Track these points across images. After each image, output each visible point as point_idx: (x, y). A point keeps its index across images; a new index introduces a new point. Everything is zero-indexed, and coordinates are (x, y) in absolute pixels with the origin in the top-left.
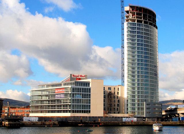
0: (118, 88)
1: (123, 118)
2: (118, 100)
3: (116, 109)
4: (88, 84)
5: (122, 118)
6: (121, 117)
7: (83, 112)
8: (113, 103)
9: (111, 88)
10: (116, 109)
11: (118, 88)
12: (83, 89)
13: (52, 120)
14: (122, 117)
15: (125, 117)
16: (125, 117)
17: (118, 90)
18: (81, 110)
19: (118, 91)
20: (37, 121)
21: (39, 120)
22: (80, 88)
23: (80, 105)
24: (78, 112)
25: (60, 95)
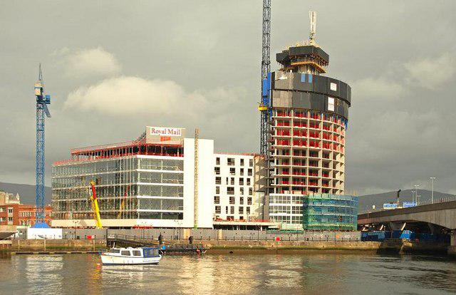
3: (245, 210)
4: (176, 150)
8: (237, 194)
10: (245, 210)
13: (93, 237)
20: (57, 238)
21: (65, 237)
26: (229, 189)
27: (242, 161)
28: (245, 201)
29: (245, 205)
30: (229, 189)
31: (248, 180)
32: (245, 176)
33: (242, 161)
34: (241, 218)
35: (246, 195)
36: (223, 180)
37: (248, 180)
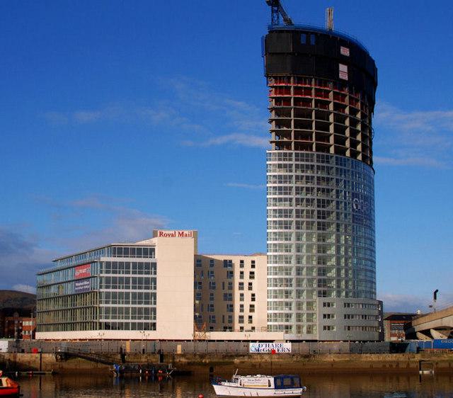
0: (253, 262)
1: (251, 344)
2: (253, 295)
5: (246, 343)
6: (244, 341)
7: (134, 327)
9: (231, 261)
11: (253, 262)
12: (134, 264)
14: (248, 341)
15: (255, 341)
16: (255, 341)
17: (253, 266)
18: (130, 321)
19: (253, 270)
22: (128, 264)
23: (128, 309)
24: (120, 327)
25: (82, 284)
26: (225, 295)
27: (242, 262)
28: (247, 308)
29: (247, 313)
30: (225, 295)
31: (250, 284)
32: (246, 280)
33: (242, 262)
34: (242, 328)
35: (247, 302)
36: (219, 286)
37: (250, 284)
